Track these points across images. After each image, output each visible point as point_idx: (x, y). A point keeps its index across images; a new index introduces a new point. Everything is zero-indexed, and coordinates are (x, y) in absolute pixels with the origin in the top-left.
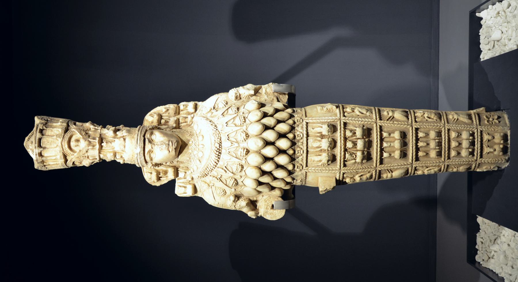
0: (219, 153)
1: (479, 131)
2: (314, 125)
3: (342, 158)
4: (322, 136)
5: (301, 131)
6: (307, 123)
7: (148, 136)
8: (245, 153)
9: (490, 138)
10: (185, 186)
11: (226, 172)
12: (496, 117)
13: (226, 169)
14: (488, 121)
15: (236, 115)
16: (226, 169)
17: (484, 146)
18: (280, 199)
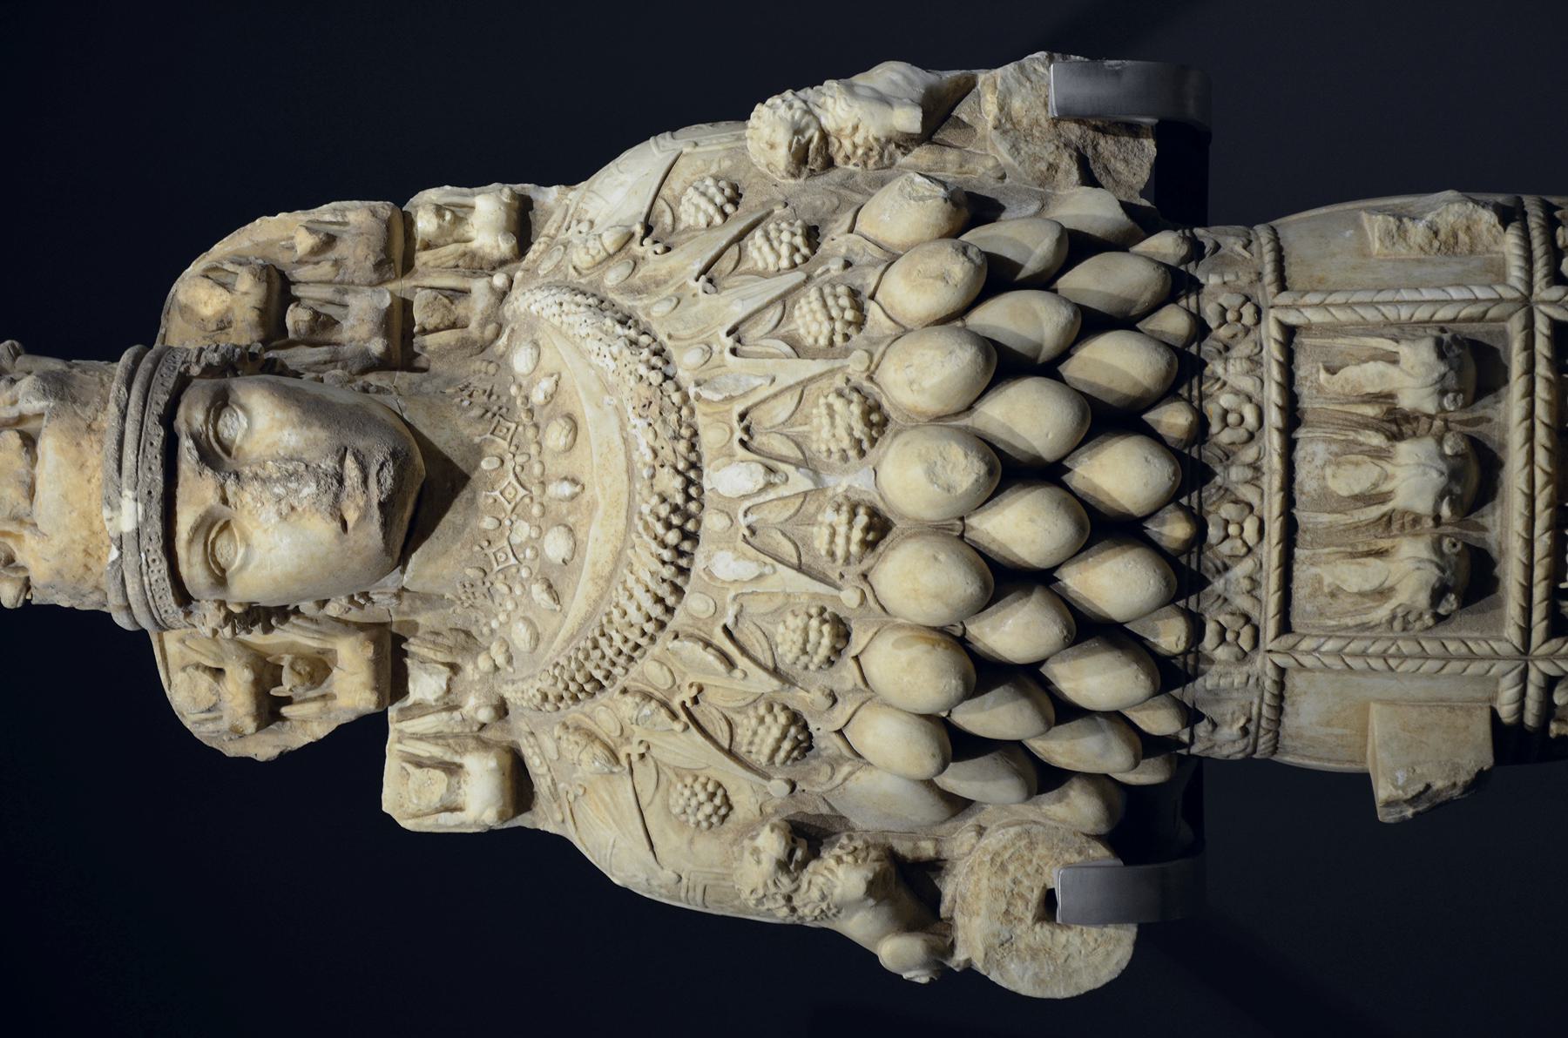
0: (683, 531)
2: (1342, 343)
3: (1539, 572)
5: (1247, 384)
6: (1289, 332)
7: (193, 415)
8: (857, 535)
10: (448, 757)
11: (730, 664)
13: (730, 646)
15: (798, 276)
16: (730, 646)
18: (1099, 852)
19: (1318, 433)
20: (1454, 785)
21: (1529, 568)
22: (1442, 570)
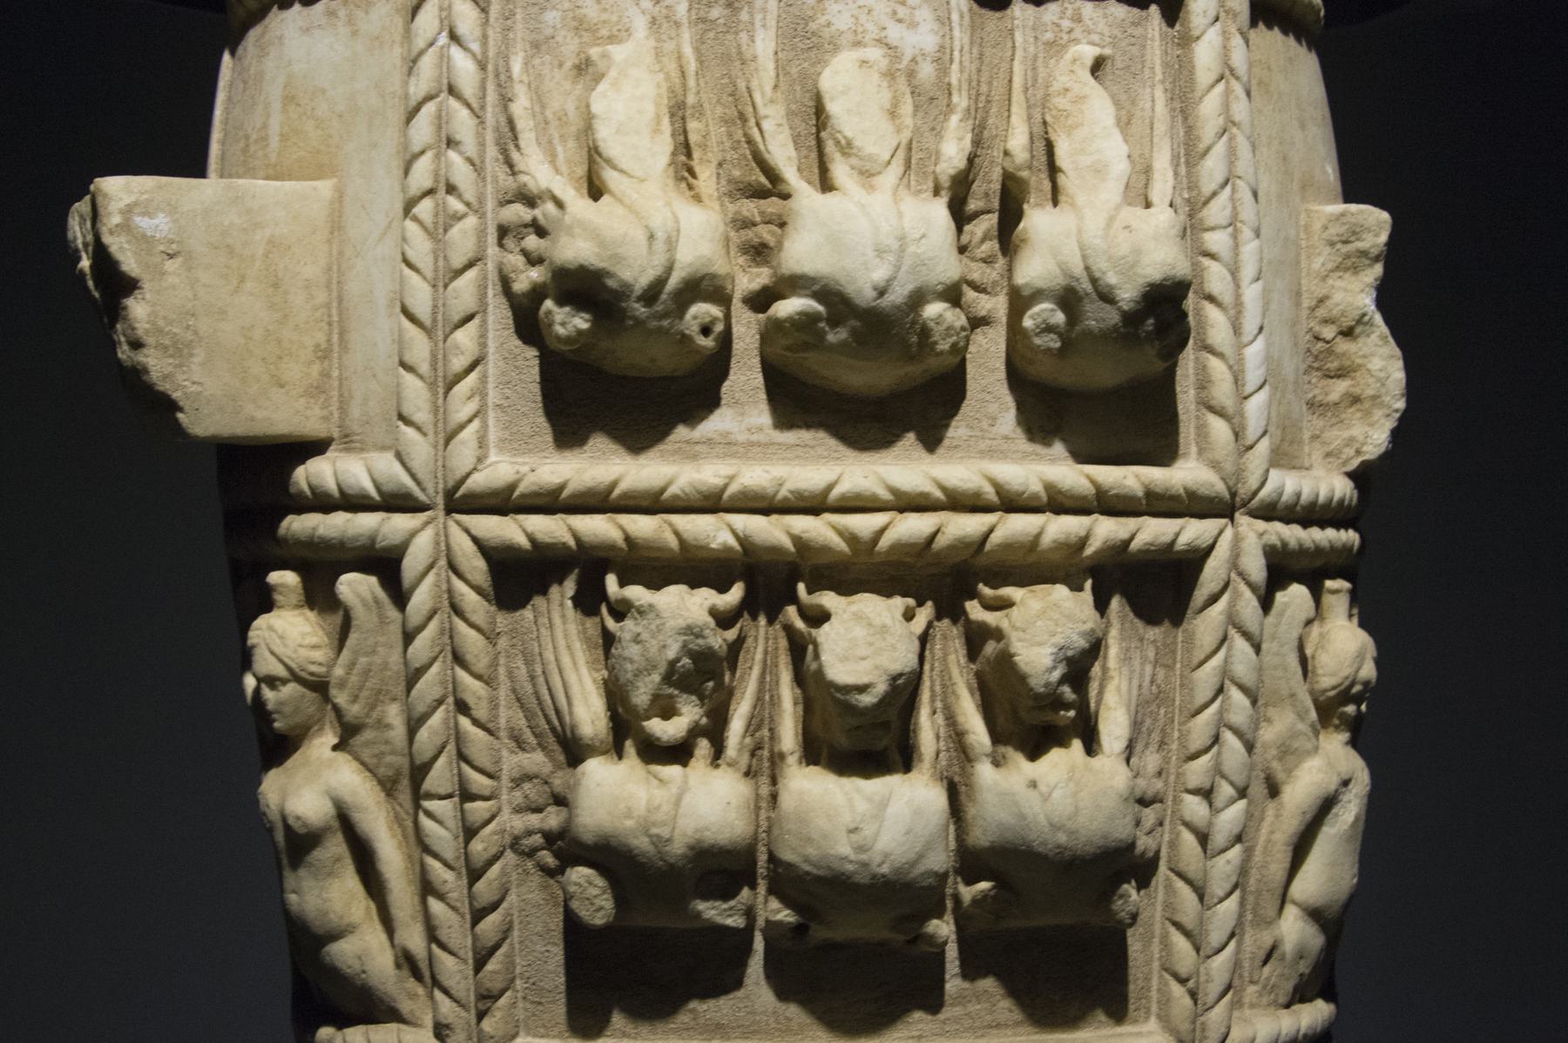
2: (1155, 102)
3: (643, 526)
4: (993, 203)
19: (960, 36)
20: (137, 345)
21: (652, 503)
22: (652, 294)
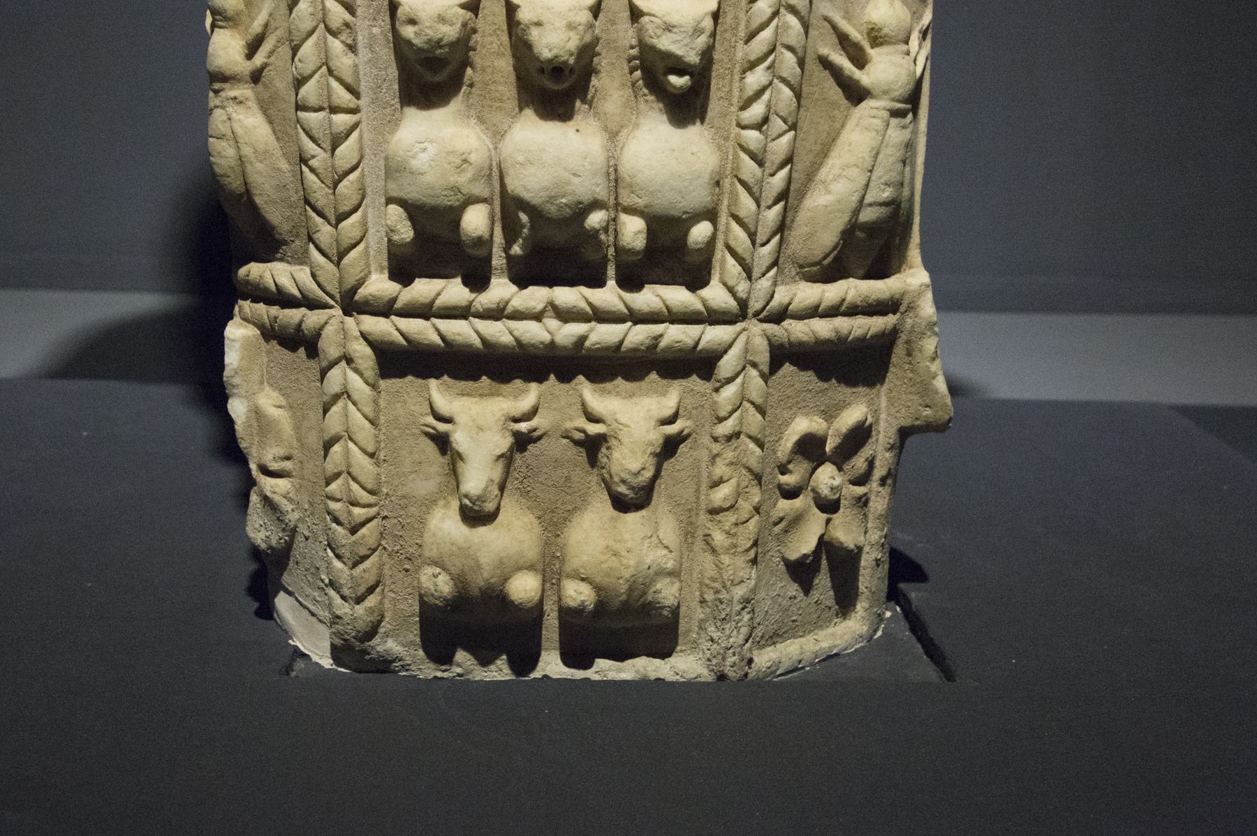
1: (714, 335)
9: (629, 459)
12: (846, 532)
14: (810, 448)
17: (530, 394)
